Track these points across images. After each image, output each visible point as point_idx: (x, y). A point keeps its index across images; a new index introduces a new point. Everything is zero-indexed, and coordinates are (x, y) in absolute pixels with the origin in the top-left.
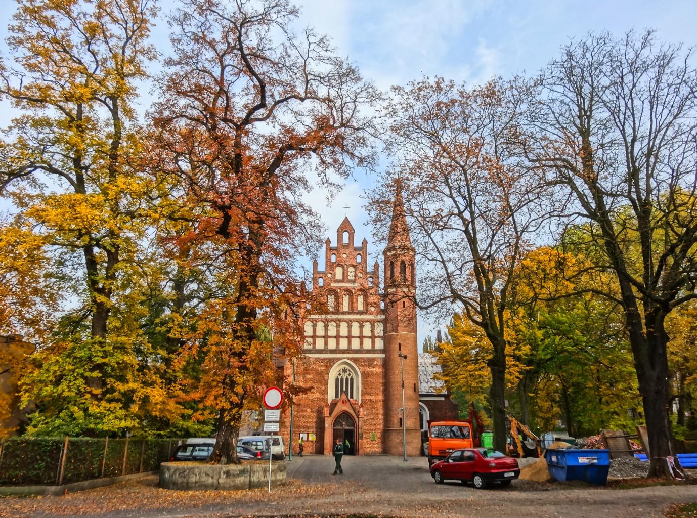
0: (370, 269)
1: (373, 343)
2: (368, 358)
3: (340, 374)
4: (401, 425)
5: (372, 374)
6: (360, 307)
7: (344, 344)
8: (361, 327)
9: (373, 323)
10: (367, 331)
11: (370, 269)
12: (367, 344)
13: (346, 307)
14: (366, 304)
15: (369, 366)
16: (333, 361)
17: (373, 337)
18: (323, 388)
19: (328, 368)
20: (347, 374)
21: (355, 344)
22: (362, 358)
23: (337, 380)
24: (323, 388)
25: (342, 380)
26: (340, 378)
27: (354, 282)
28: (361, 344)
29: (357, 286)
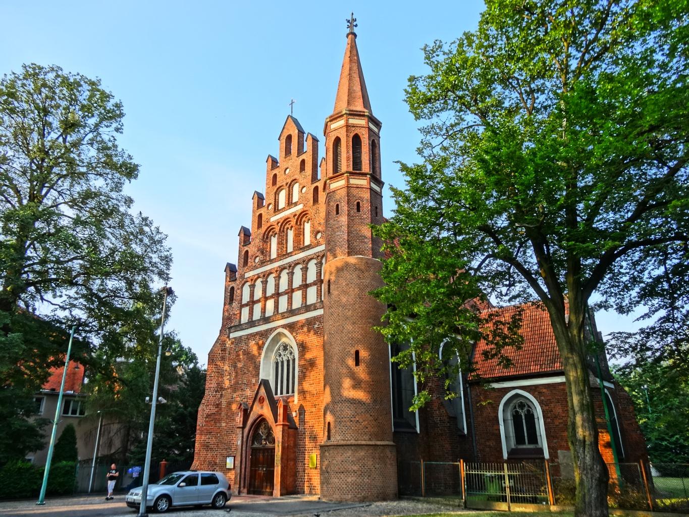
23: (277, 363)
25: (282, 362)
26: (280, 360)
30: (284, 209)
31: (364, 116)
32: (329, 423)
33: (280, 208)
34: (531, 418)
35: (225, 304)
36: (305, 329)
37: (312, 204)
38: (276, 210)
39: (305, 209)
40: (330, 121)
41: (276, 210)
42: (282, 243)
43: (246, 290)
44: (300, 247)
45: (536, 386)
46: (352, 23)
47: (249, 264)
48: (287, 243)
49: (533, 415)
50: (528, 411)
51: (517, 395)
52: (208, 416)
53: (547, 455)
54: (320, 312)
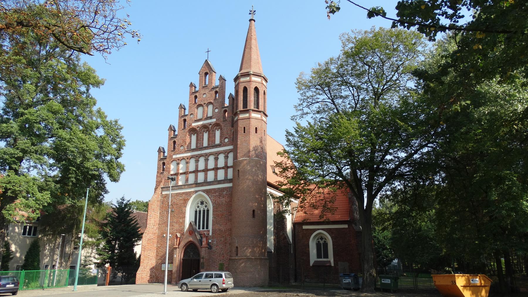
1: (226, 174)
2: (219, 189)
3: (198, 207)
6: (217, 142)
7: (201, 177)
8: (216, 159)
9: (226, 154)
11: (227, 103)
12: (221, 175)
16: (189, 194)
17: (226, 167)
18: (181, 221)
19: (186, 201)
20: (204, 206)
21: (211, 176)
23: (196, 212)
24: (181, 221)
25: (200, 211)
27: (211, 118)
28: (216, 175)
29: (214, 120)
31: (260, 76)
34: (326, 245)
36: (217, 194)
37: (222, 120)
39: (218, 122)
40: (241, 76)
42: (199, 140)
44: (212, 145)
45: (330, 229)
47: (176, 150)
48: (203, 140)
49: (327, 244)
50: (325, 241)
51: (320, 233)
52: (149, 240)
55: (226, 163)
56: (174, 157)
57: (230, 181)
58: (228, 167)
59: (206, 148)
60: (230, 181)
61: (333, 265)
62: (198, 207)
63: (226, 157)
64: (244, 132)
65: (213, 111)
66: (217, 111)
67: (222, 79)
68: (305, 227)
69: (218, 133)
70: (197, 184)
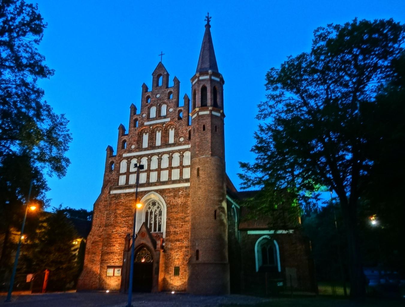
0: (182, 103)
1: (181, 173)
2: (173, 189)
4: (197, 258)
5: (177, 204)
10: (176, 163)
11: (182, 103)
13: (158, 143)
14: (176, 135)
15: (175, 196)
17: (181, 167)
20: (155, 207)
22: (169, 189)
23: (147, 213)
25: (151, 213)
26: (149, 211)
27: (165, 117)
30: (153, 119)
32: (197, 251)
33: (151, 117)
35: (106, 172)
36: (172, 194)
38: (149, 118)
41: (149, 118)
42: (152, 139)
43: (124, 164)
44: (165, 144)
46: (208, 19)
53: (280, 270)
54: (187, 185)
55: (181, 162)
56: (125, 155)
57: (187, 181)
58: (183, 167)
59: (159, 147)
60: (187, 181)
61: (280, 270)
62: (149, 208)
63: (182, 157)
64: (204, 129)
65: (167, 111)
66: (171, 110)
67: (177, 82)
68: (250, 232)
69: (172, 133)
70: (148, 184)
